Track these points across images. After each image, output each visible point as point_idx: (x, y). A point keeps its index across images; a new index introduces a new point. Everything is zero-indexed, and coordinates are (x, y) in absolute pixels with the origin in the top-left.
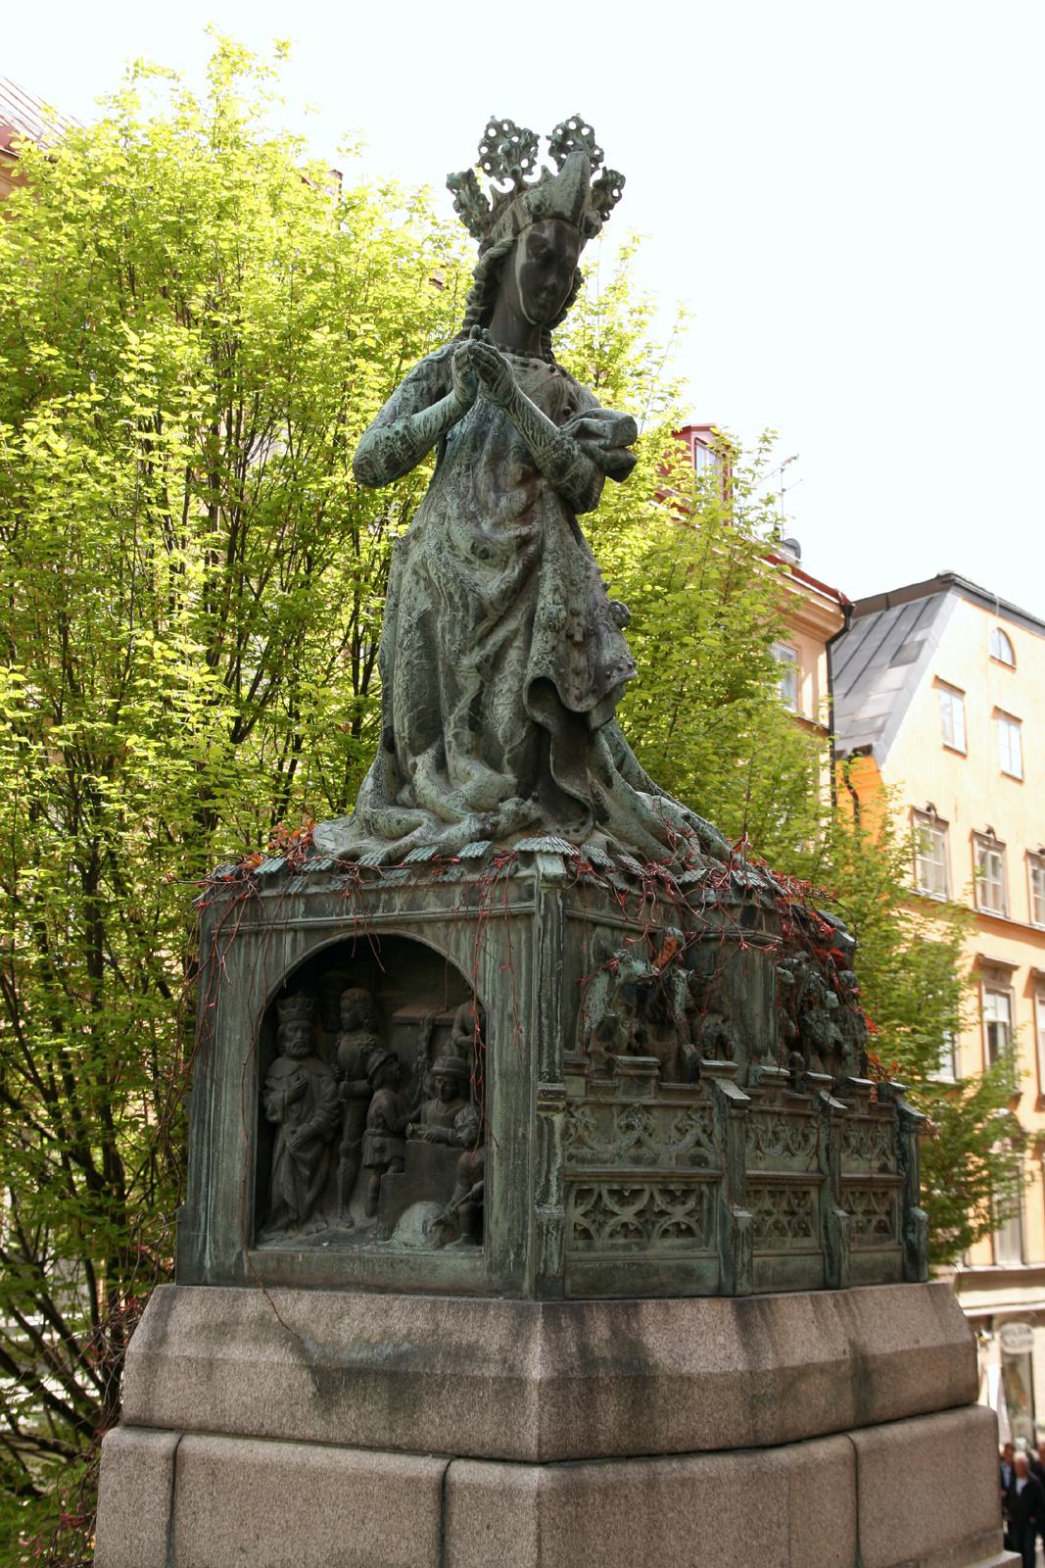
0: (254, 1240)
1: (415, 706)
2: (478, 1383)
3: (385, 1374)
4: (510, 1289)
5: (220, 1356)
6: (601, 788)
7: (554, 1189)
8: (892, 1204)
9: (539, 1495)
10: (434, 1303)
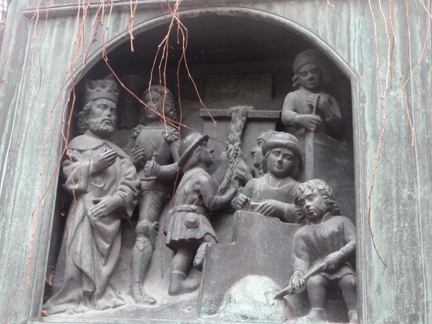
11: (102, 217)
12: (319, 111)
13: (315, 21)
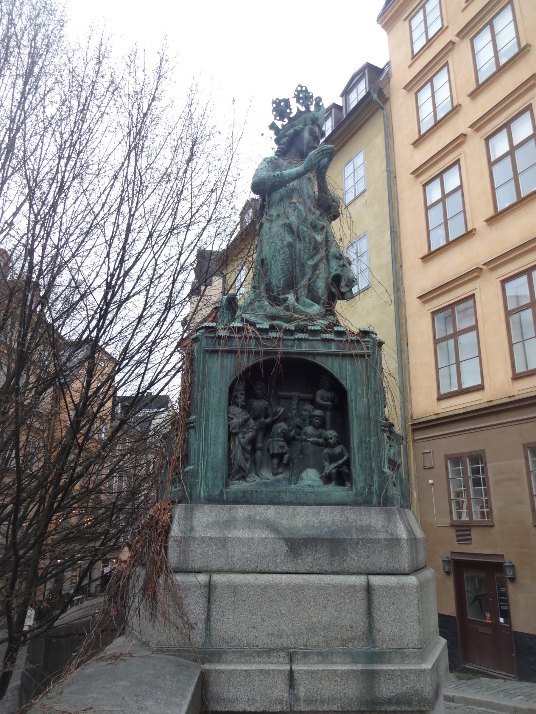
0: (227, 486)
1: (286, 276)
2: (376, 541)
3: (327, 540)
4: (367, 503)
5: (229, 536)
10: (342, 510)
11: (246, 444)
12: (332, 401)
13: (333, 366)
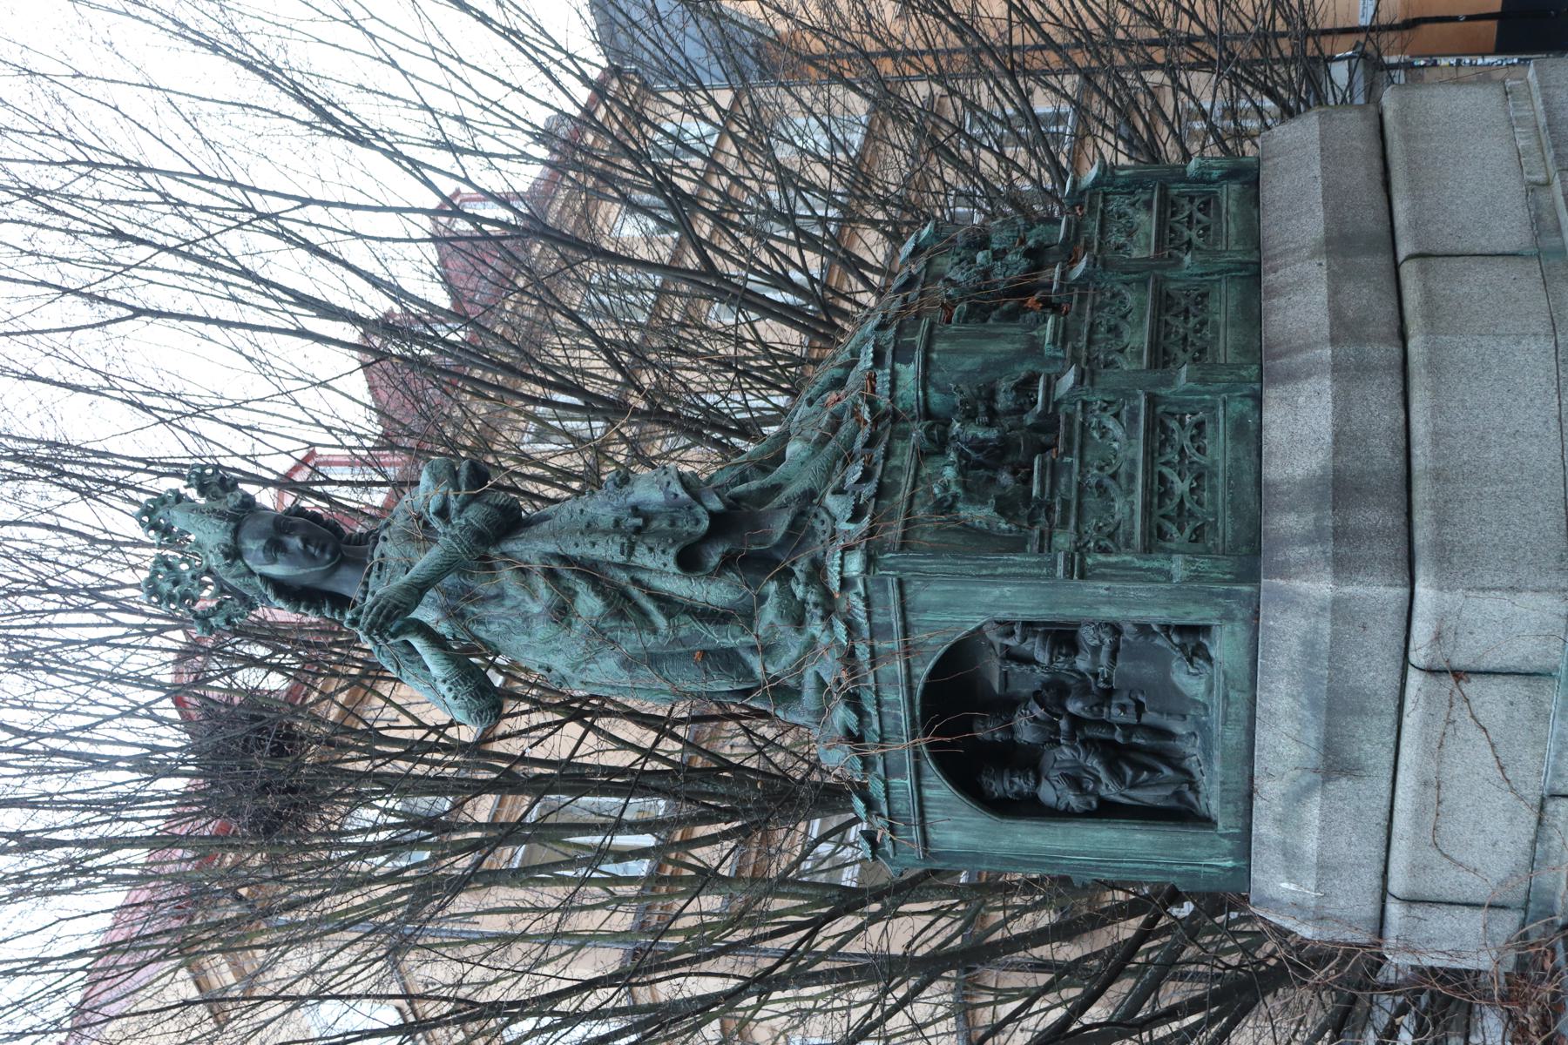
2: (1336, 639)
6: (781, 498)
7: (1156, 564)
8: (1182, 195)
9: (1441, 589)
